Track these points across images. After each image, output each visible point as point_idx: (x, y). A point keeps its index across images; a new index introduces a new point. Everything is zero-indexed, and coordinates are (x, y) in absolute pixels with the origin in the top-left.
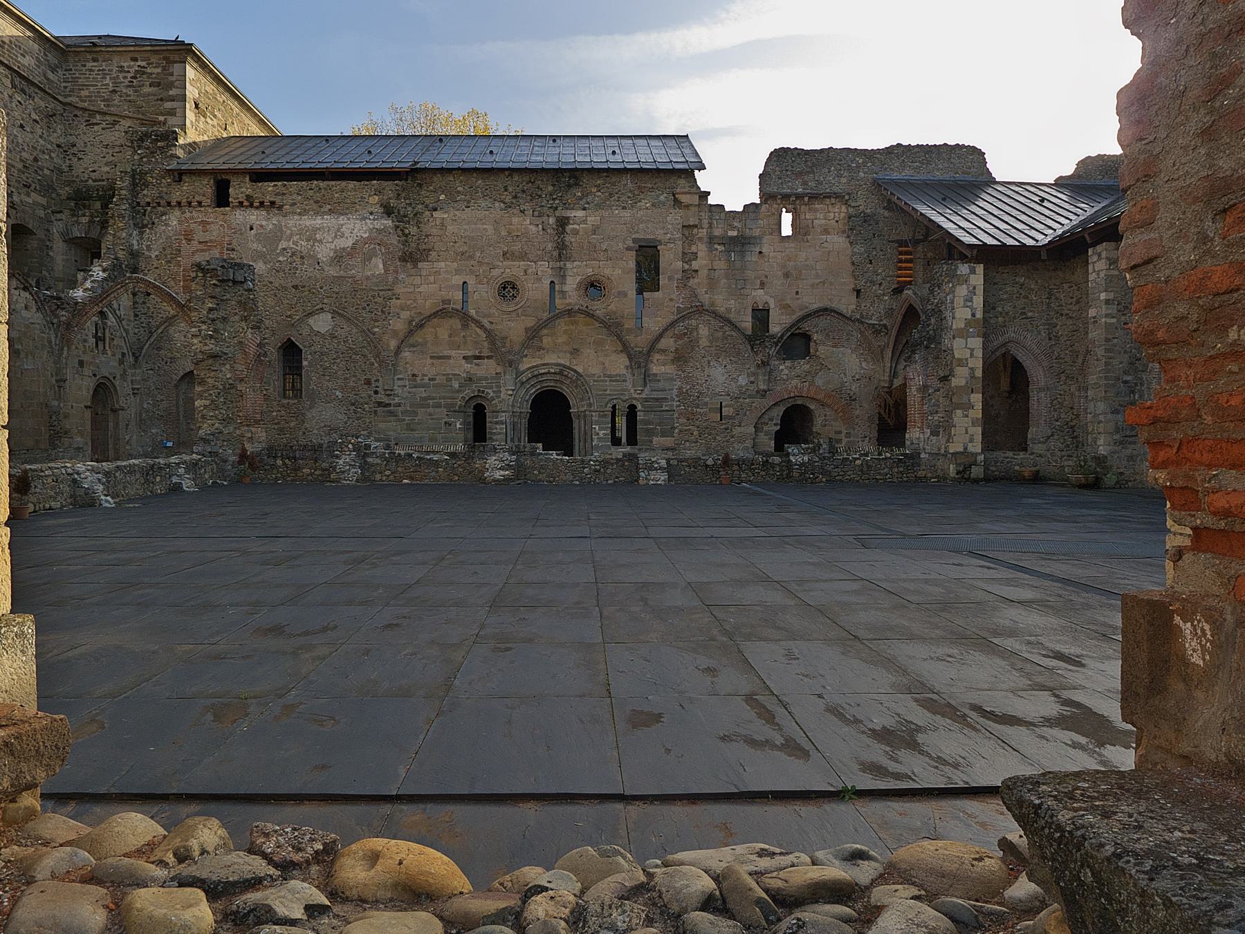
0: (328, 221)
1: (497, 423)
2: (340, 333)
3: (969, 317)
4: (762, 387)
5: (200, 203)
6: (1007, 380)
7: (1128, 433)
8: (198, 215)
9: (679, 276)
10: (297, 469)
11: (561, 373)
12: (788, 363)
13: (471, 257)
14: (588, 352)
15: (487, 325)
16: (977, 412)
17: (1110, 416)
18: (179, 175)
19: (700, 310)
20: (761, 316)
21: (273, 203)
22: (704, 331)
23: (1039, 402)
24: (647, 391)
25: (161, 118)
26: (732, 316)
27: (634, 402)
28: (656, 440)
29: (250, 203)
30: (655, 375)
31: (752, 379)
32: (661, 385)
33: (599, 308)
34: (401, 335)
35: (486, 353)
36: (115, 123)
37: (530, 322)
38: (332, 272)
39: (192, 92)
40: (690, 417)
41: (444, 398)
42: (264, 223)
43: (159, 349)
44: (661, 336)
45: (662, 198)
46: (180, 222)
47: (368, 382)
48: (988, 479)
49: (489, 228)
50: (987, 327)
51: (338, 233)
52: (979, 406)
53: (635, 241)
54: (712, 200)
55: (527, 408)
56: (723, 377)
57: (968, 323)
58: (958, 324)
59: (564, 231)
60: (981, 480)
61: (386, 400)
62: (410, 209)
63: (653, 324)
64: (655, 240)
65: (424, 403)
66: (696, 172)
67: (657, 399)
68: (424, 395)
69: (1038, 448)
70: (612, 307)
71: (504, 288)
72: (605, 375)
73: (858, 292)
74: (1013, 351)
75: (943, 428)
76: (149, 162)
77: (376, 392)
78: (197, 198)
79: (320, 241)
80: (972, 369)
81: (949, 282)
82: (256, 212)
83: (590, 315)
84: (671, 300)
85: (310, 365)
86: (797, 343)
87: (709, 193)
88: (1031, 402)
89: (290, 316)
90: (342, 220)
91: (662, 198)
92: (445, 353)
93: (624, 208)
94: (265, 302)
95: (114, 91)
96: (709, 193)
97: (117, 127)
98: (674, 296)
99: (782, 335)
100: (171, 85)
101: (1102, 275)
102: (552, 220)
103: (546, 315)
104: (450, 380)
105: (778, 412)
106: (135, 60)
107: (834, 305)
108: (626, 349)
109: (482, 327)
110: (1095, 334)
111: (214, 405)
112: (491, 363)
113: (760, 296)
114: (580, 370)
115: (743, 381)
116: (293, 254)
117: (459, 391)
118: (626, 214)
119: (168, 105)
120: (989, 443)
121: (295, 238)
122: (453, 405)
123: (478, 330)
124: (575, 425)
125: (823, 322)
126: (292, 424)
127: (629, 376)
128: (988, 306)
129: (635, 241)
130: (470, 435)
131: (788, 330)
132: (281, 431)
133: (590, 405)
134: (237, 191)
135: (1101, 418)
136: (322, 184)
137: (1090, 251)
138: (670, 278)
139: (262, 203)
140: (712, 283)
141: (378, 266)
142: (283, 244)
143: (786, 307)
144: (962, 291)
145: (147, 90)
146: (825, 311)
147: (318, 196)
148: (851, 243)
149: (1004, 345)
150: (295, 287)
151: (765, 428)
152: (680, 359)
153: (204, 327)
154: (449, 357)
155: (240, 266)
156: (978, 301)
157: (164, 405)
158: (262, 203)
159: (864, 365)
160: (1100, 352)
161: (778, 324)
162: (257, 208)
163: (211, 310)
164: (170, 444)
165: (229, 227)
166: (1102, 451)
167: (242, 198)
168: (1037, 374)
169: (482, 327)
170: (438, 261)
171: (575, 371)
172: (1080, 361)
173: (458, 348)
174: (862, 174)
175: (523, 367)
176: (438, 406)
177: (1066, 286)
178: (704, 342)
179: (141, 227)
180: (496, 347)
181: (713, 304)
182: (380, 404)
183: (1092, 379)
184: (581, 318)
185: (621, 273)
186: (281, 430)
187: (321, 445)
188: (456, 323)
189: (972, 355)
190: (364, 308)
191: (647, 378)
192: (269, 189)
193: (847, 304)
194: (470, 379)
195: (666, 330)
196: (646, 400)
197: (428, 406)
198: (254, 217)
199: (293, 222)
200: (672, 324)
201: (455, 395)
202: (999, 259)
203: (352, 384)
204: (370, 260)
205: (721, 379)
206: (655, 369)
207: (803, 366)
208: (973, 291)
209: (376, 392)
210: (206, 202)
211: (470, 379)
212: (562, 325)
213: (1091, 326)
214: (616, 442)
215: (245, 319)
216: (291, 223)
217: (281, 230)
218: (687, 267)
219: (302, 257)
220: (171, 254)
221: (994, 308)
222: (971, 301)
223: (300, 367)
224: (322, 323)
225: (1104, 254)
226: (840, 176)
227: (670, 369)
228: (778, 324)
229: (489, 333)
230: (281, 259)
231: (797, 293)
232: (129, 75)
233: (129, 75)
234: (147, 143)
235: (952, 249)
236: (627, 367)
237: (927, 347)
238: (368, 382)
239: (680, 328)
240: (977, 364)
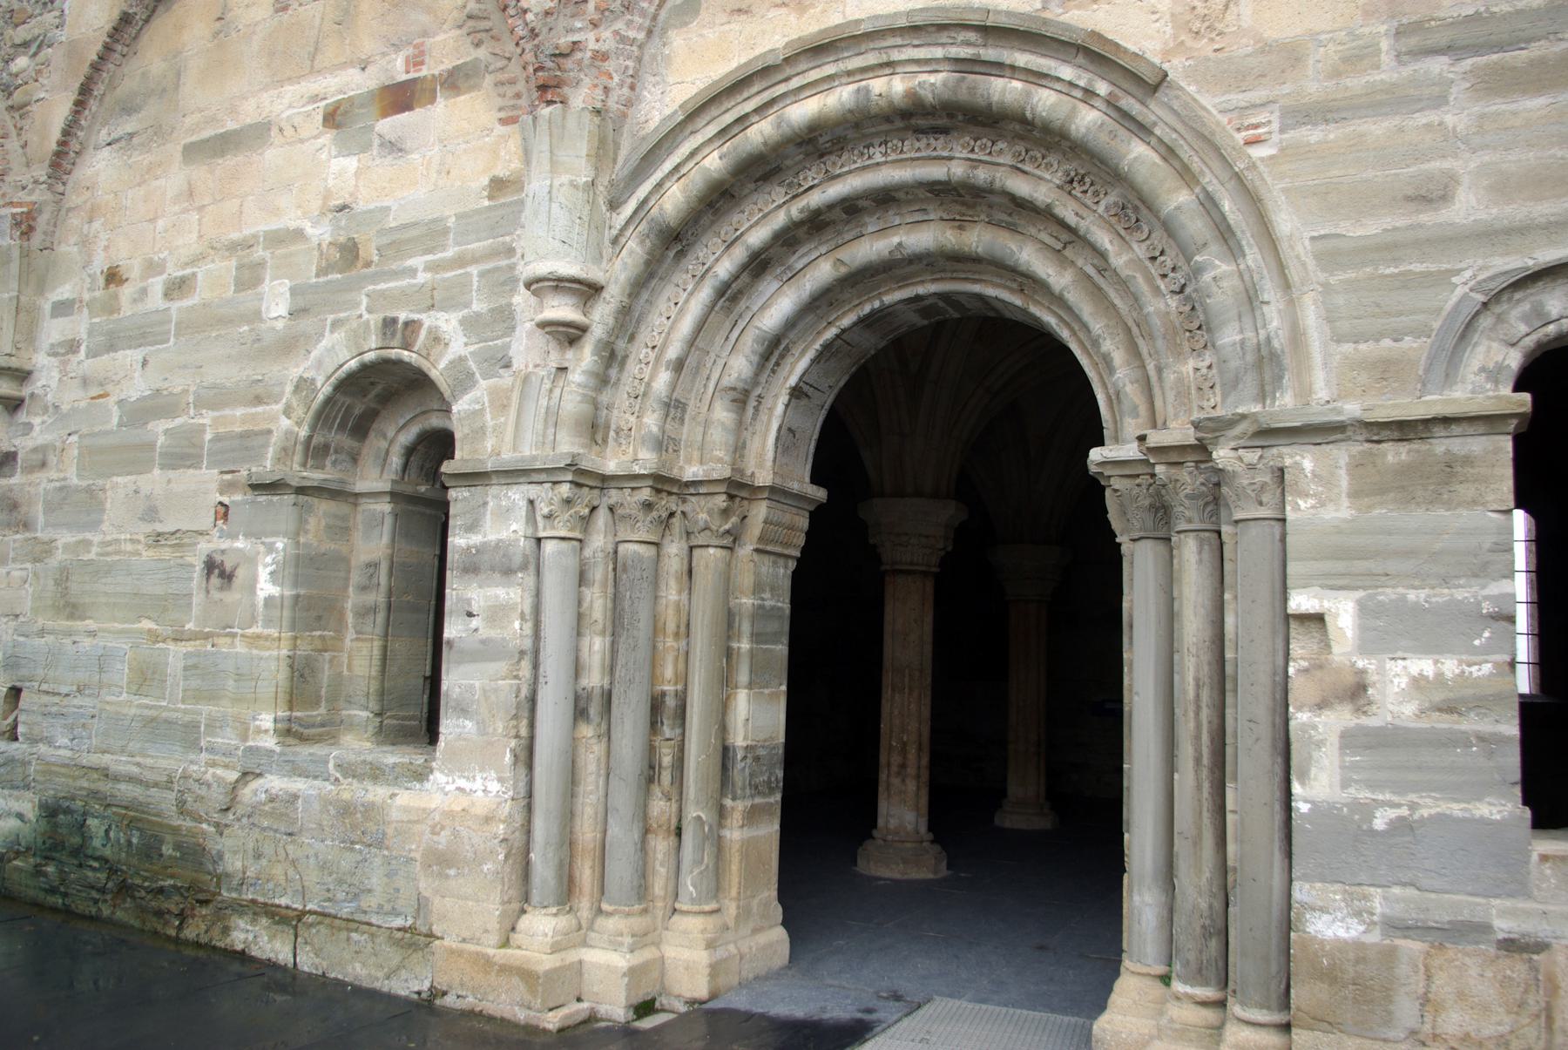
41: (217, 398)
68: (137, 388)
92: (249, 113)
104: (250, 277)
122: (249, 442)
124: (1141, 568)
133: (1268, 365)
171: (1094, 53)
175: (661, 104)
176: (183, 456)
211: (349, 253)
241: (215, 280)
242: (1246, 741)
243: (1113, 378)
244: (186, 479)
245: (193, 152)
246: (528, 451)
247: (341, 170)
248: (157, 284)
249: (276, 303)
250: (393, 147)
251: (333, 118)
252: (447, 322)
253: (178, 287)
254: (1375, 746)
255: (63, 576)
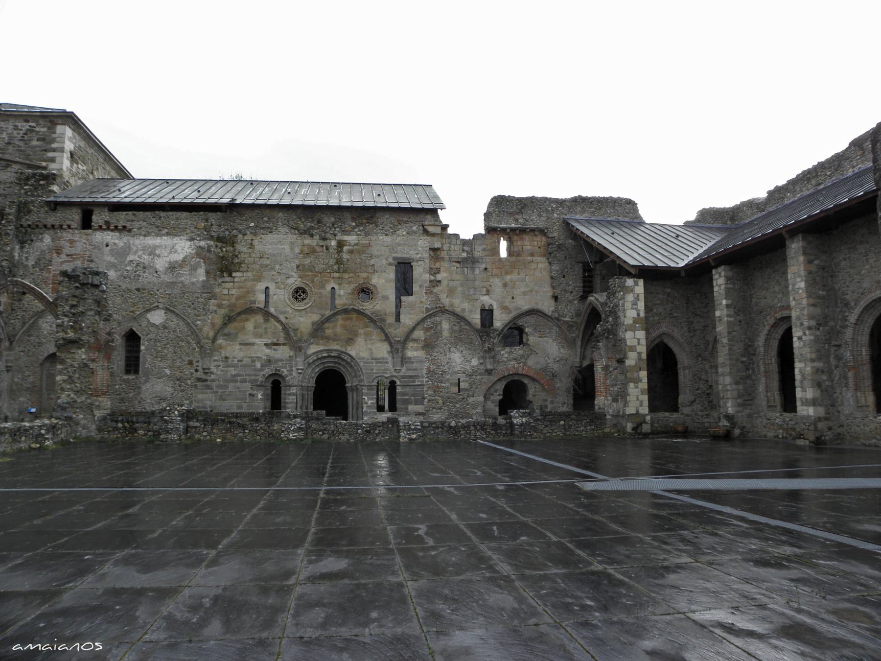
0: (166, 241)
1: (290, 394)
2: (172, 325)
3: (636, 316)
4: (489, 367)
5: (69, 226)
6: (662, 361)
7: (747, 398)
8: (67, 235)
9: (427, 284)
10: (136, 430)
11: (338, 357)
12: (507, 349)
13: (273, 269)
14: (360, 340)
15: (283, 320)
16: (644, 384)
17: (734, 386)
18: (55, 206)
19: (443, 311)
20: (487, 314)
21: (124, 227)
22: (445, 326)
23: (684, 377)
24: (404, 370)
25: (44, 164)
26: (466, 315)
27: (394, 379)
28: (411, 408)
29: (107, 227)
30: (410, 358)
31: (481, 361)
32: (414, 365)
33: (368, 307)
34: (217, 327)
35: (282, 341)
36: (8, 166)
37: (316, 317)
38: (167, 278)
39: (69, 146)
40: (436, 390)
41: (249, 375)
42: (117, 241)
43: (29, 336)
44: (413, 329)
45: (415, 228)
46: (53, 240)
47: (190, 363)
48: (654, 433)
49: (287, 247)
50: (647, 323)
51: (173, 250)
52: (645, 380)
53: (394, 258)
54: (450, 231)
55: (312, 383)
56: (460, 361)
57: (635, 321)
58: (628, 321)
59: (341, 251)
60: (650, 434)
61: (204, 377)
62: (227, 233)
63: (408, 319)
64: (409, 258)
65: (233, 379)
66: (439, 211)
67: (411, 377)
68: (234, 373)
69: (686, 410)
70: (378, 307)
71: (297, 292)
72: (372, 359)
73: (556, 298)
74: (666, 341)
75: (621, 396)
76: (33, 196)
77: (197, 371)
78: (68, 222)
79: (159, 256)
80: (640, 354)
81: (620, 292)
82: (111, 233)
83: (359, 312)
84: (421, 302)
85: (147, 349)
86: (515, 334)
87: (447, 226)
88: (680, 377)
89: (132, 312)
90: (176, 240)
91: (415, 228)
92: (252, 340)
93: (387, 235)
94: (114, 302)
95: (9, 143)
96: (447, 226)
97: (9, 169)
98: (423, 300)
99: (502, 330)
100: (54, 141)
101: (723, 287)
102: (334, 243)
103: (328, 313)
104: (253, 361)
105: (501, 386)
106: (27, 121)
107: (540, 307)
108: (387, 338)
109: (279, 321)
110: (721, 328)
111: (70, 380)
112: (286, 348)
113: (486, 300)
114: (353, 353)
115: (475, 362)
116: (138, 265)
117: (261, 370)
118: (388, 239)
119: (50, 154)
120: (653, 408)
121: (140, 253)
123: (276, 324)
124: (350, 396)
125: (531, 319)
126: (131, 395)
127: (390, 359)
128: (648, 309)
129: (394, 258)
130: (269, 404)
131: (506, 325)
132: (122, 400)
133: (362, 381)
134: (98, 218)
135: (729, 387)
136: (163, 214)
137: (714, 272)
138: (421, 286)
139: (116, 227)
140: (451, 292)
141: (201, 275)
142: (131, 257)
143: (505, 308)
144: (630, 297)
145: (35, 143)
146: (532, 312)
147: (159, 223)
148: (550, 263)
149: (659, 336)
150: (138, 290)
151: (492, 398)
152: (428, 346)
153: (66, 319)
154: (253, 344)
155: (97, 274)
156: (641, 305)
157: (31, 379)
158: (116, 227)
159: (562, 350)
160: (725, 341)
161: (500, 321)
162: (112, 230)
163: (73, 306)
164: (33, 410)
165: (90, 245)
166: (730, 411)
167: (101, 222)
168: (683, 358)
169: (279, 321)
170: (247, 271)
172: (710, 346)
173: (261, 337)
174: (555, 215)
176: (244, 381)
177: (698, 295)
178: (446, 334)
179: (22, 243)
180: (291, 337)
181: (452, 305)
182: (199, 380)
183: (720, 360)
184: (354, 316)
185: (384, 282)
186: (122, 400)
187: (153, 413)
188: (260, 318)
189: (639, 344)
190: (190, 307)
191: (404, 360)
192: (121, 218)
193: (548, 306)
194: (269, 361)
195: (418, 324)
196: (403, 377)
197: (236, 381)
198: (110, 237)
199: (139, 242)
200: (423, 320)
201: (258, 373)
202: (651, 275)
203: (178, 364)
204: (195, 270)
205: (459, 361)
206: (410, 354)
207: (518, 351)
208: (637, 298)
209: (197, 371)
210: (74, 225)
211: (269, 361)
212: (340, 320)
213: (717, 323)
214: (381, 409)
215: (99, 313)
216: (137, 242)
217: (129, 248)
218: (432, 278)
219: (144, 268)
220: (43, 263)
221: (651, 310)
222: (636, 304)
223: (139, 351)
224: (157, 317)
225: (723, 274)
226: (540, 216)
227: (421, 354)
228: (500, 321)
229: (285, 328)
230: (128, 268)
231: (513, 298)
232: (22, 132)
233: (22, 132)
234: (32, 181)
235: (620, 269)
236: (389, 352)
237: (607, 338)
238: (190, 363)
239: (428, 323)
240: (643, 349)
241: (246, 361)
242: (359, 405)
243: (348, 378)
244: (244, 384)
245: (240, 344)
246: (296, 384)
247: (267, 351)
248: (236, 360)
249: (258, 365)
250: (275, 350)
251: (265, 344)
252: (284, 370)
253: (241, 361)
254: (368, 407)
255: (220, 396)
